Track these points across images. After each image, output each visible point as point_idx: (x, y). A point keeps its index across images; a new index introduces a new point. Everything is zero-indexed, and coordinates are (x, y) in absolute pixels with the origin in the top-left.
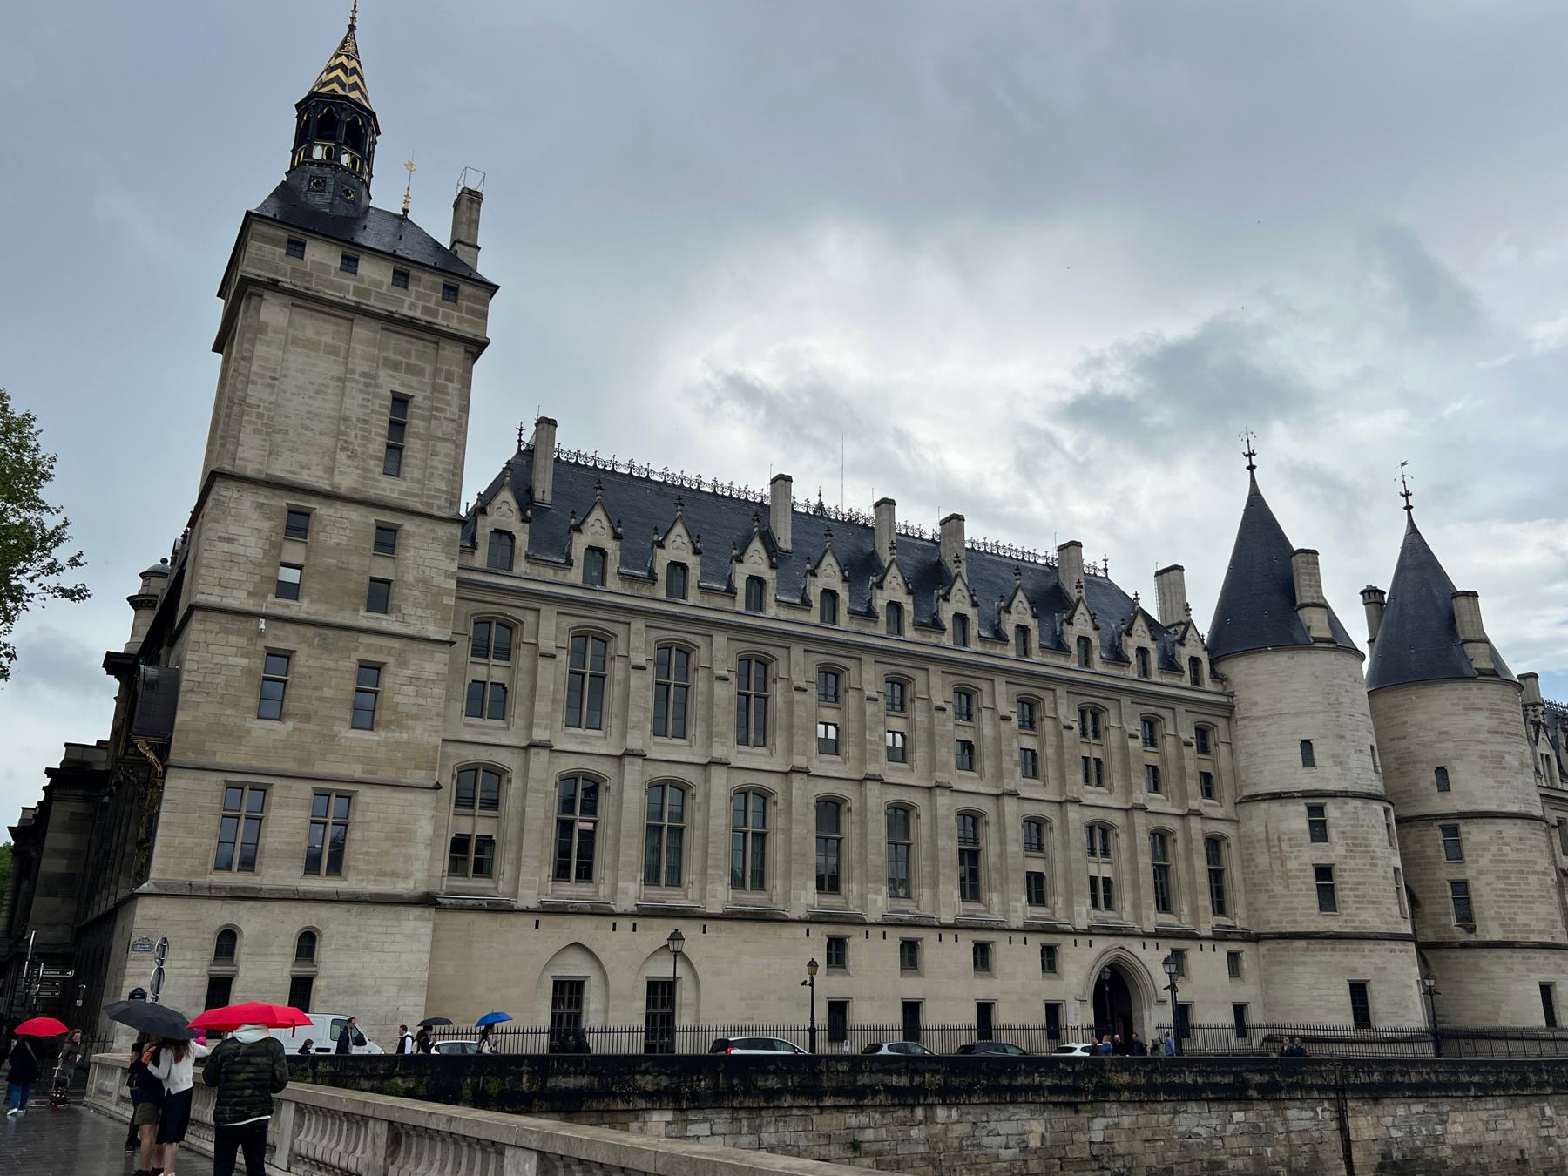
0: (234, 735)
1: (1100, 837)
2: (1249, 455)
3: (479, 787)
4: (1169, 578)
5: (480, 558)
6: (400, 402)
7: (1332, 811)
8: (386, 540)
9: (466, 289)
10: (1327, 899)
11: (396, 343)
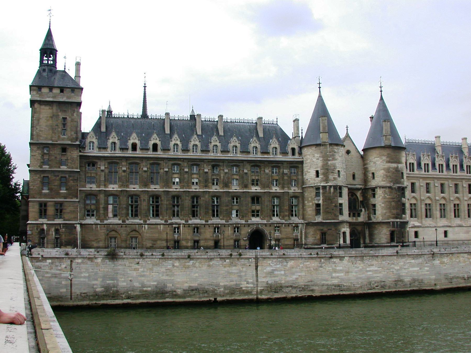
4: (296, 121)
7: (321, 191)
10: (318, 212)
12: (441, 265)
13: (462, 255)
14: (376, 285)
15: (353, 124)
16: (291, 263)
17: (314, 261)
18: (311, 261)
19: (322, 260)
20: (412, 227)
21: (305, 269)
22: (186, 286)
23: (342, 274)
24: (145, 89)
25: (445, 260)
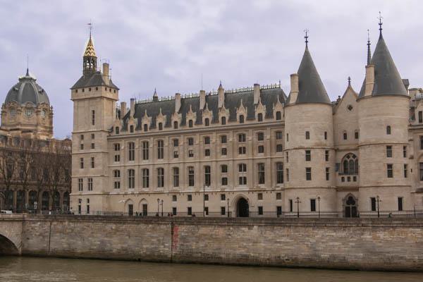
0: (78, 172)
1: (242, 167)
2: (306, 37)
3: (117, 173)
5: (114, 133)
6: (94, 111)
8: (93, 136)
9: (99, 87)
11: (91, 101)
12: (374, 241)
13: (411, 229)
14: (286, 258)
15: (342, 73)
16: (203, 230)
17: (223, 229)
18: (220, 229)
19: (231, 228)
20: (417, 192)
21: (214, 237)
22: (119, 246)
23: (250, 244)
24: (369, 47)
25: (382, 235)
